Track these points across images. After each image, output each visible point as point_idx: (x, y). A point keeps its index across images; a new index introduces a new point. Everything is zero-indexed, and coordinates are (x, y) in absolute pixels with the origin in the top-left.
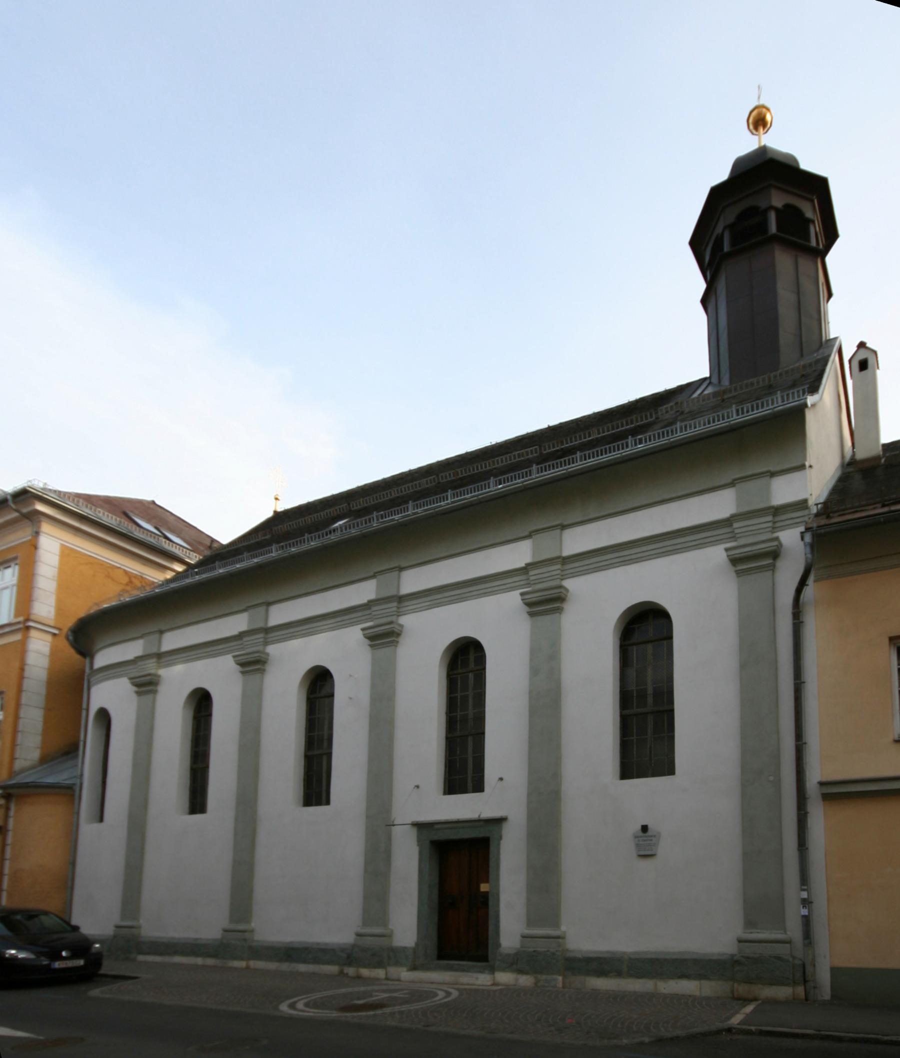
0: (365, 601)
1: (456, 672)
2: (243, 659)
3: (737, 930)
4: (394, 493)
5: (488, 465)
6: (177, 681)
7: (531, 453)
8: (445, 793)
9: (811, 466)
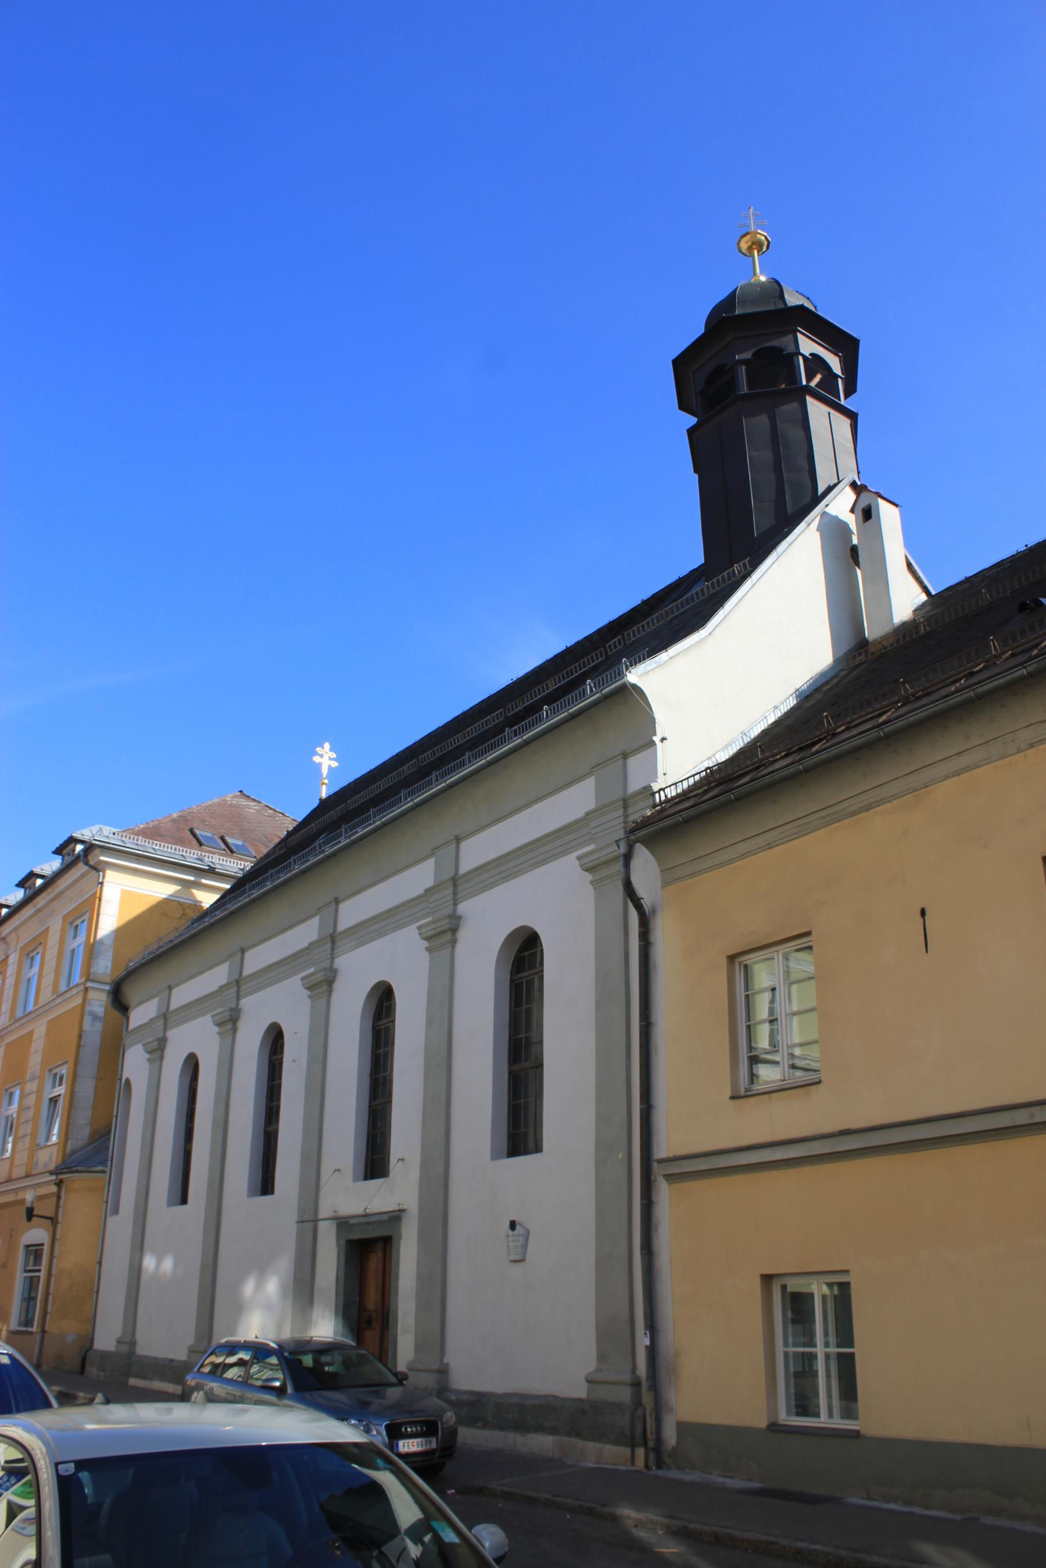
0: (306, 945)
1: (520, 975)
2: (219, 1021)
3: (590, 1364)
4: (382, 785)
5: (459, 739)
6: (358, 973)
7: (495, 718)
8: (366, 1178)
9: (663, 739)
